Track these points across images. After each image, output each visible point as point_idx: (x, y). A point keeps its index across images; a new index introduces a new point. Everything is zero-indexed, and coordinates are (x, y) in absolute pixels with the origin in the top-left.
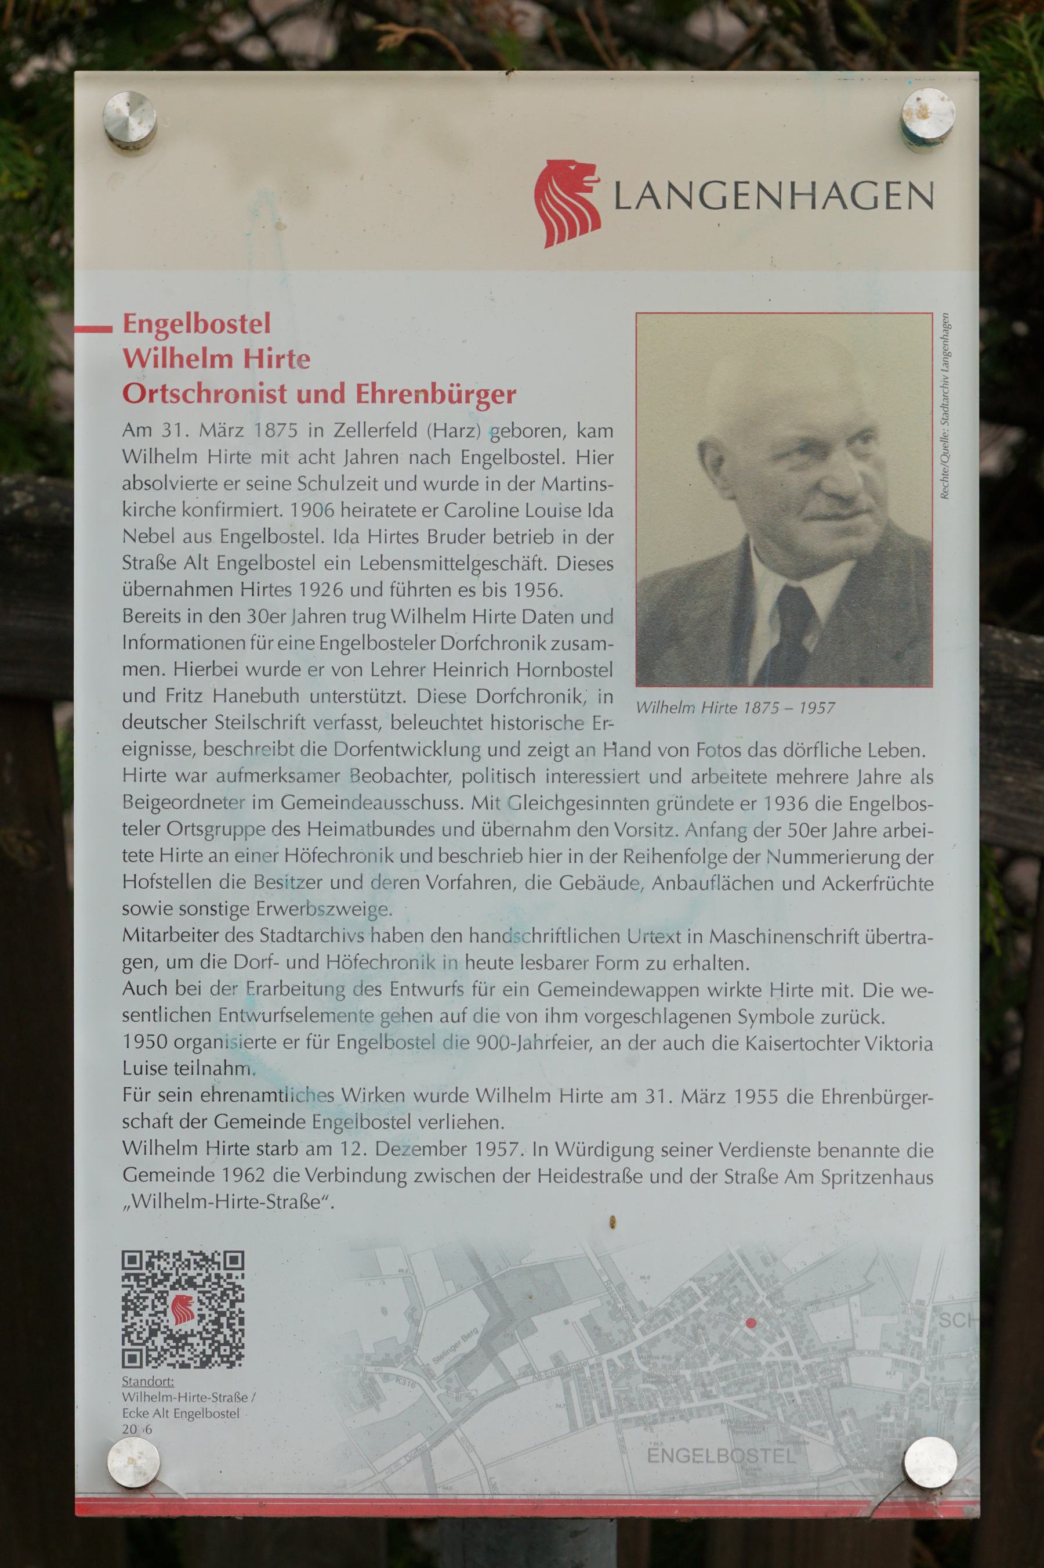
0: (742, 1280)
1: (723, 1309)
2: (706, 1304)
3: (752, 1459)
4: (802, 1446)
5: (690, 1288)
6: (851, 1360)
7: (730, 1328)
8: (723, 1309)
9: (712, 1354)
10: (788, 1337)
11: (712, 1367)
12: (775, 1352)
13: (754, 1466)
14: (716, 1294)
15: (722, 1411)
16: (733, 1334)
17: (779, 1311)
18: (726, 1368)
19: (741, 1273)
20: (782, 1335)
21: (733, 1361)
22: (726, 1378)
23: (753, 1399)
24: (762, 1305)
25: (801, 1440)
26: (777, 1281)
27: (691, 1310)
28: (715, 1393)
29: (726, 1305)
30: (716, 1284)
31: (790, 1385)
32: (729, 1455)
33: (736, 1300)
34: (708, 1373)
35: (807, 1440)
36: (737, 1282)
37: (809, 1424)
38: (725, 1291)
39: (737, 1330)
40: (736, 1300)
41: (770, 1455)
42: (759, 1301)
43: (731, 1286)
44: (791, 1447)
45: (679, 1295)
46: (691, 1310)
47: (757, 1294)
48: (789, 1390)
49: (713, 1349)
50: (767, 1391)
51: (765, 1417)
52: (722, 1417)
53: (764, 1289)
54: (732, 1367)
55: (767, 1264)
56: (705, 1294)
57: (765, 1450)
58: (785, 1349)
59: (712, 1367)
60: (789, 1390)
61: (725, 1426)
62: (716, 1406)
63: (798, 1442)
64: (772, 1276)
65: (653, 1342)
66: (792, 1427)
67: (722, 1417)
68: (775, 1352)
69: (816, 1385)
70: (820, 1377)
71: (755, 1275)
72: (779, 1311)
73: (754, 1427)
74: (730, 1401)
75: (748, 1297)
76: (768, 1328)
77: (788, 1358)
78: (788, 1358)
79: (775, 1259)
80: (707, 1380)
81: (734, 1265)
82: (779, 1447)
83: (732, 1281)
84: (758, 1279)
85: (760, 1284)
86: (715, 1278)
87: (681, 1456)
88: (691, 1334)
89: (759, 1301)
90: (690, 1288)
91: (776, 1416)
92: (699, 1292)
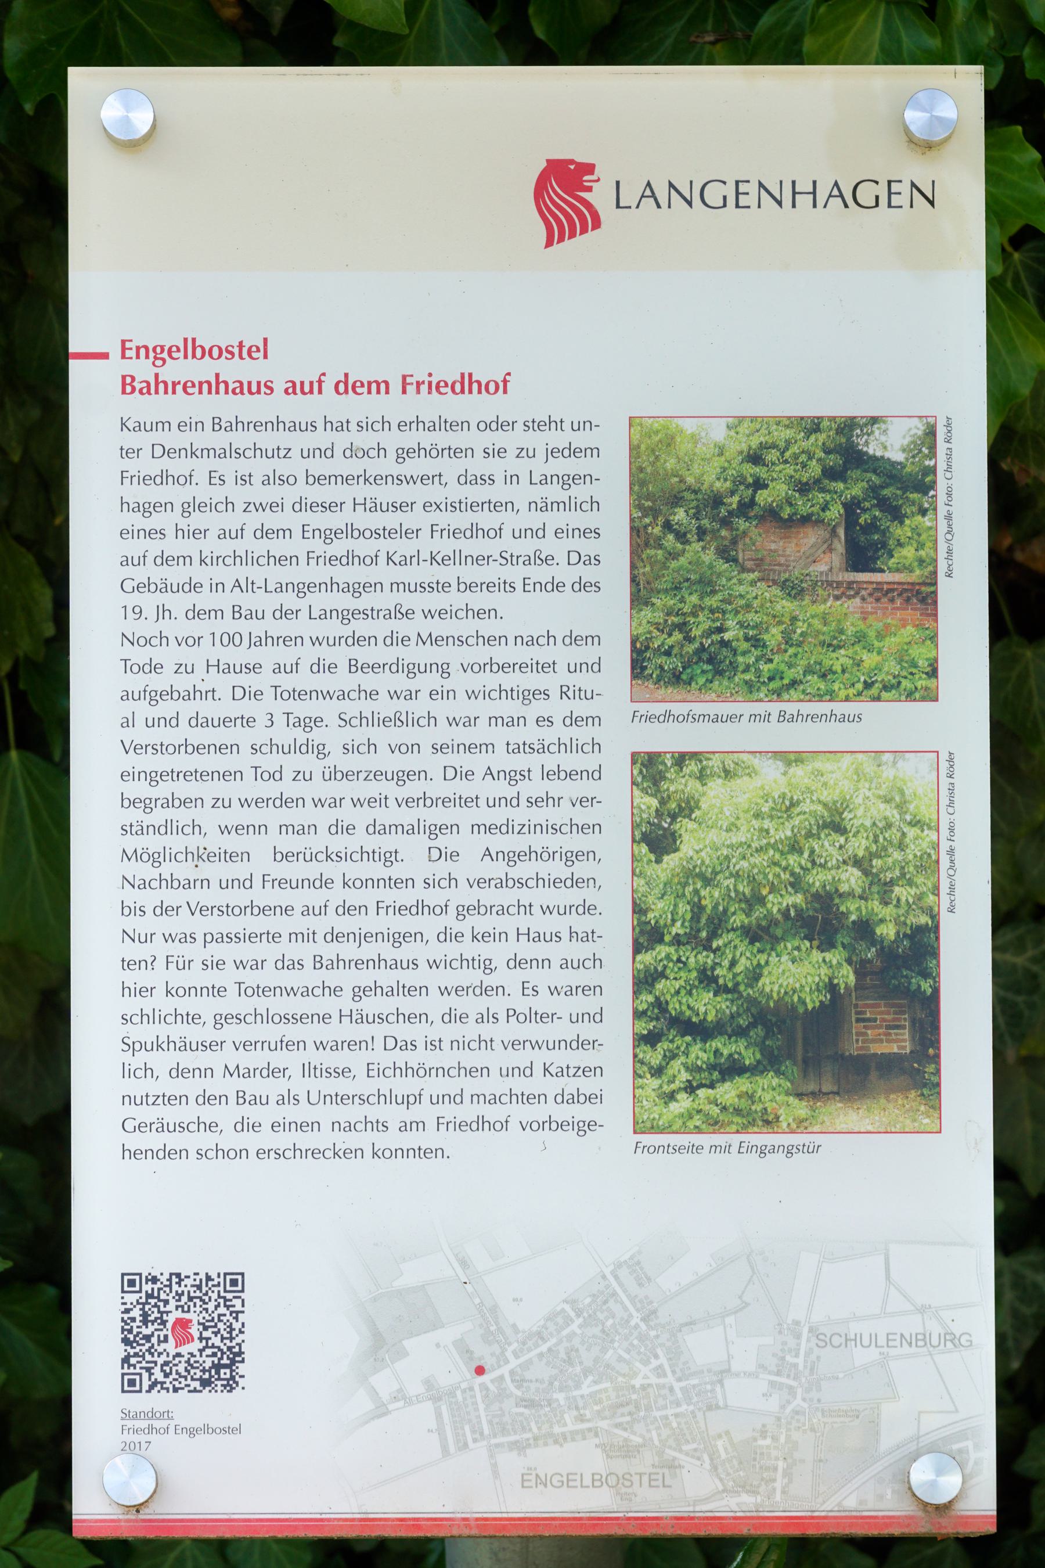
0: (616, 1301)
1: (596, 1331)
2: (580, 1327)
3: (627, 1483)
4: (678, 1471)
5: (563, 1310)
6: (726, 1382)
7: (604, 1350)
8: (596, 1331)
9: (586, 1376)
10: (663, 1360)
11: (586, 1389)
12: (649, 1374)
13: (630, 1490)
14: (590, 1316)
15: (596, 1435)
16: (607, 1356)
17: (653, 1333)
18: (600, 1391)
19: (614, 1294)
20: (656, 1357)
21: (608, 1385)
22: (600, 1402)
23: (628, 1423)
24: (637, 1326)
25: (676, 1463)
26: (651, 1302)
27: (565, 1333)
28: (588, 1416)
29: (600, 1327)
30: (590, 1305)
31: (665, 1407)
32: (604, 1480)
33: (610, 1322)
34: (582, 1396)
35: (682, 1463)
36: (611, 1304)
37: (685, 1448)
38: (598, 1313)
39: (611, 1352)
40: (610, 1322)
41: (645, 1479)
42: (633, 1323)
43: (604, 1307)
44: (666, 1471)
45: (551, 1317)
46: (565, 1333)
47: (631, 1316)
48: (664, 1413)
49: (586, 1372)
50: (642, 1414)
51: (640, 1440)
52: (597, 1441)
53: (638, 1310)
54: (606, 1390)
55: (640, 1285)
56: (578, 1316)
57: (641, 1474)
58: (659, 1371)
59: (586, 1389)
60: (664, 1413)
61: (599, 1450)
62: (590, 1430)
63: (673, 1466)
64: (646, 1297)
65: (527, 1365)
66: (667, 1451)
67: (597, 1441)
68: (649, 1374)
69: (691, 1408)
70: (695, 1399)
71: (628, 1296)
72: (653, 1333)
73: (628, 1451)
74: (604, 1424)
75: (622, 1319)
76: (642, 1350)
77: (662, 1381)
78: (662, 1381)
79: (649, 1279)
80: (581, 1404)
81: (607, 1287)
82: (654, 1471)
83: (605, 1302)
84: (633, 1299)
85: (634, 1304)
86: (588, 1300)
87: (555, 1483)
88: (565, 1357)
89: (633, 1323)
90: (563, 1310)
91: (651, 1439)
92: (572, 1314)
